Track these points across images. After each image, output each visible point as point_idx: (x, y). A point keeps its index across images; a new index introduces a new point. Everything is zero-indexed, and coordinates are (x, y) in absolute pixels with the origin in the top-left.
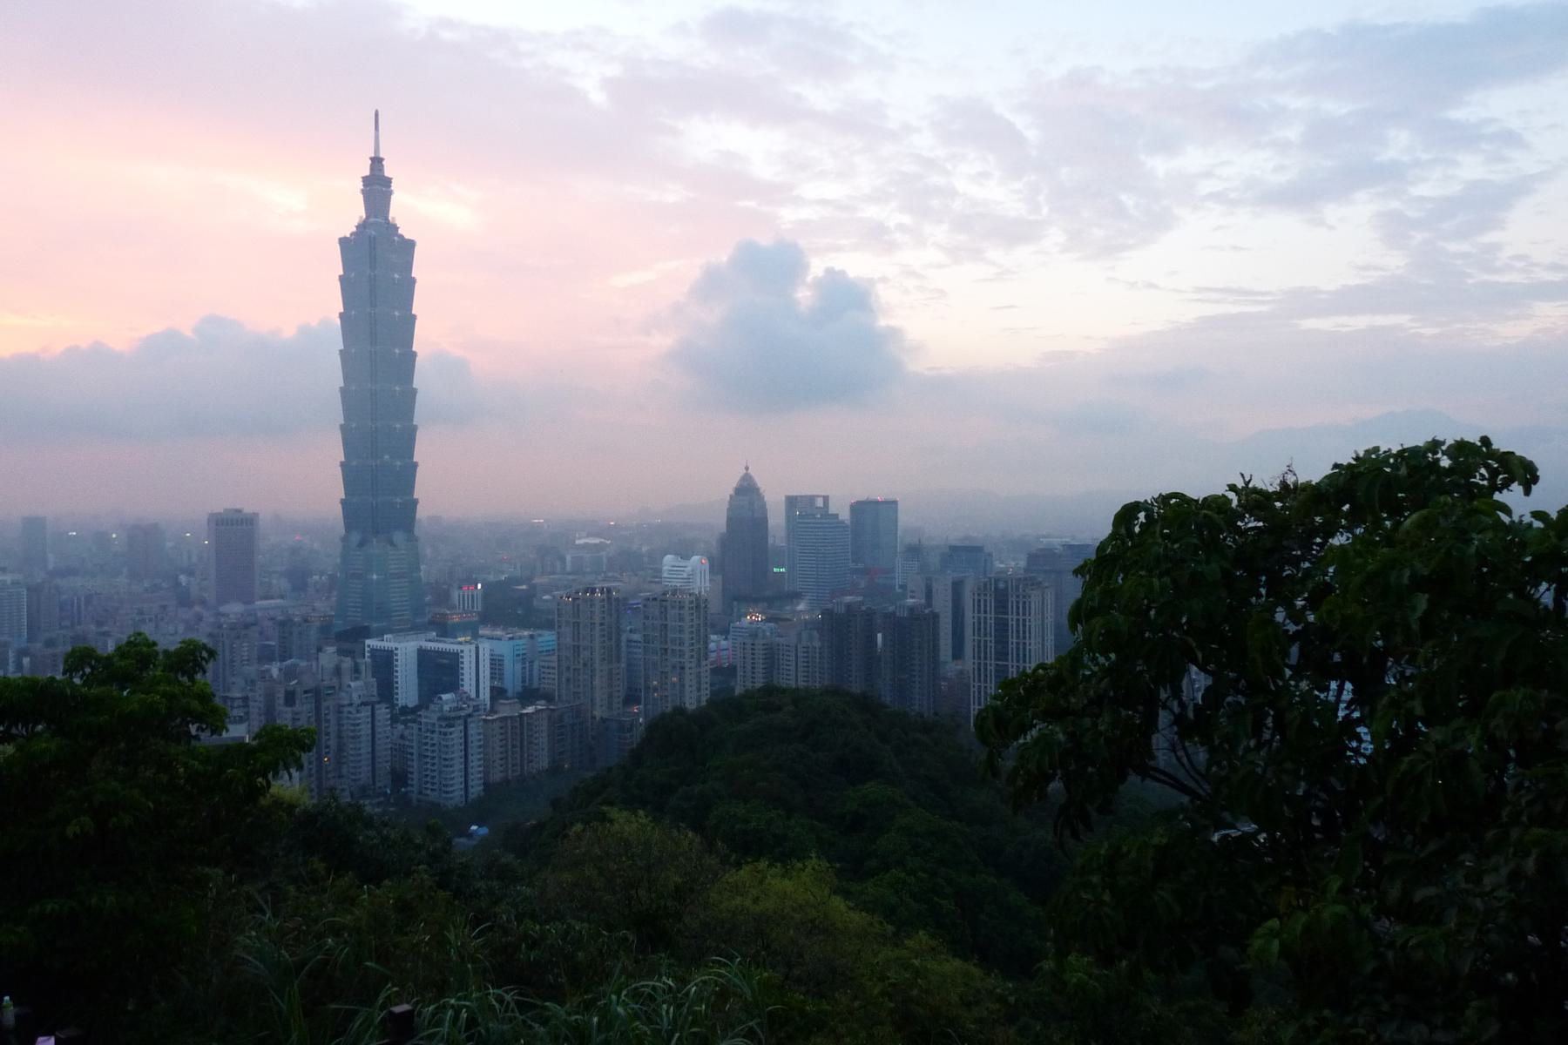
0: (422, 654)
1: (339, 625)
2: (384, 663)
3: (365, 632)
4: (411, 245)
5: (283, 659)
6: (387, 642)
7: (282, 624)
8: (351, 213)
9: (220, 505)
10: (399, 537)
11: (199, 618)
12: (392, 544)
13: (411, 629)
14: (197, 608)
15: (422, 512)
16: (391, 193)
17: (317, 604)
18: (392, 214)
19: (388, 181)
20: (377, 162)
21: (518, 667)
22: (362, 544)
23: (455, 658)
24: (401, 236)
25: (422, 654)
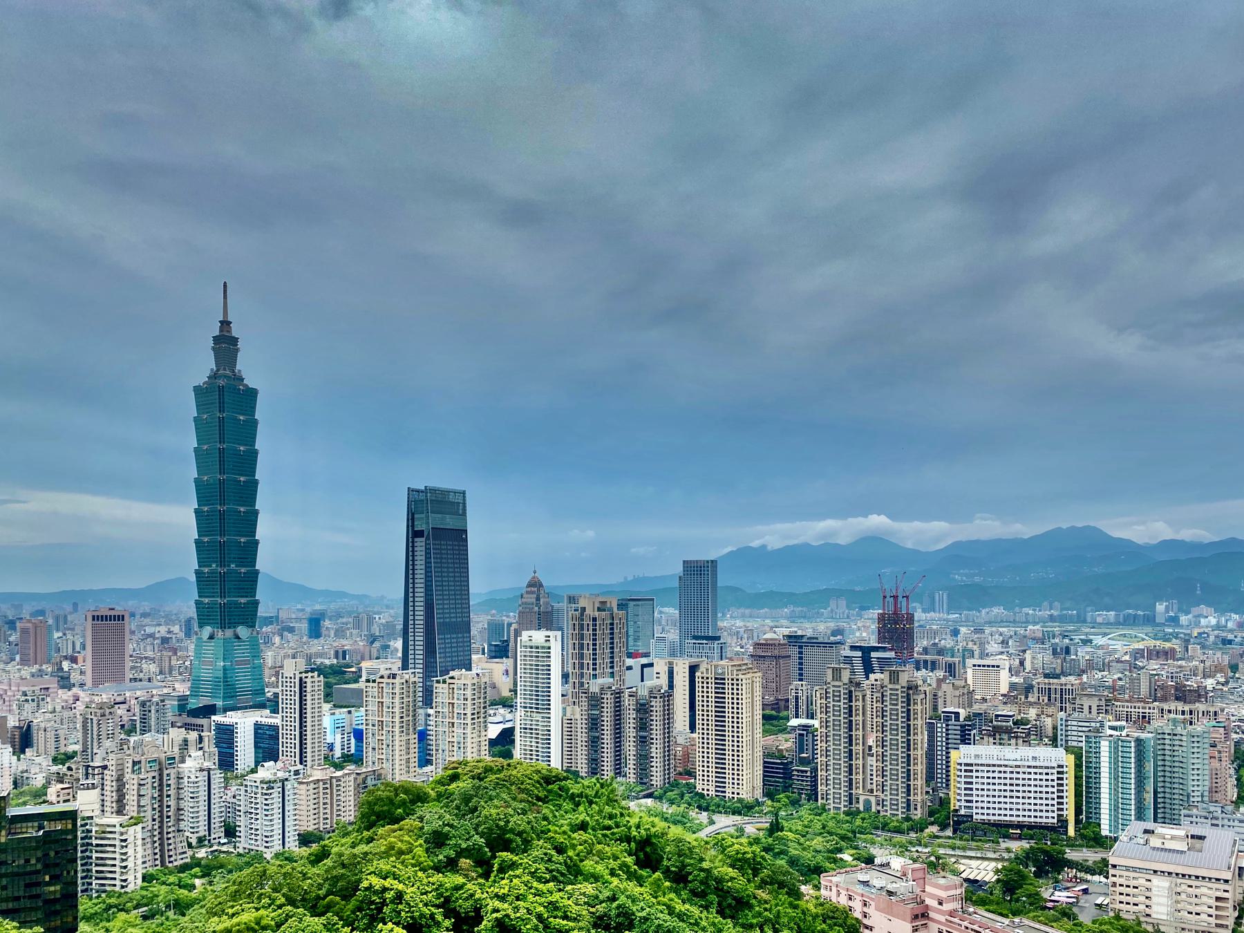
0: (258, 727)
1: (194, 703)
2: (226, 736)
3: (209, 710)
5: (143, 732)
6: (230, 718)
7: (143, 704)
10: (242, 631)
12: (238, 637)
13: (251, 707)
14: (75, 690)
15: (262, 612)
17: (177, 686)
21: (339, 736)
22: (211, 637)
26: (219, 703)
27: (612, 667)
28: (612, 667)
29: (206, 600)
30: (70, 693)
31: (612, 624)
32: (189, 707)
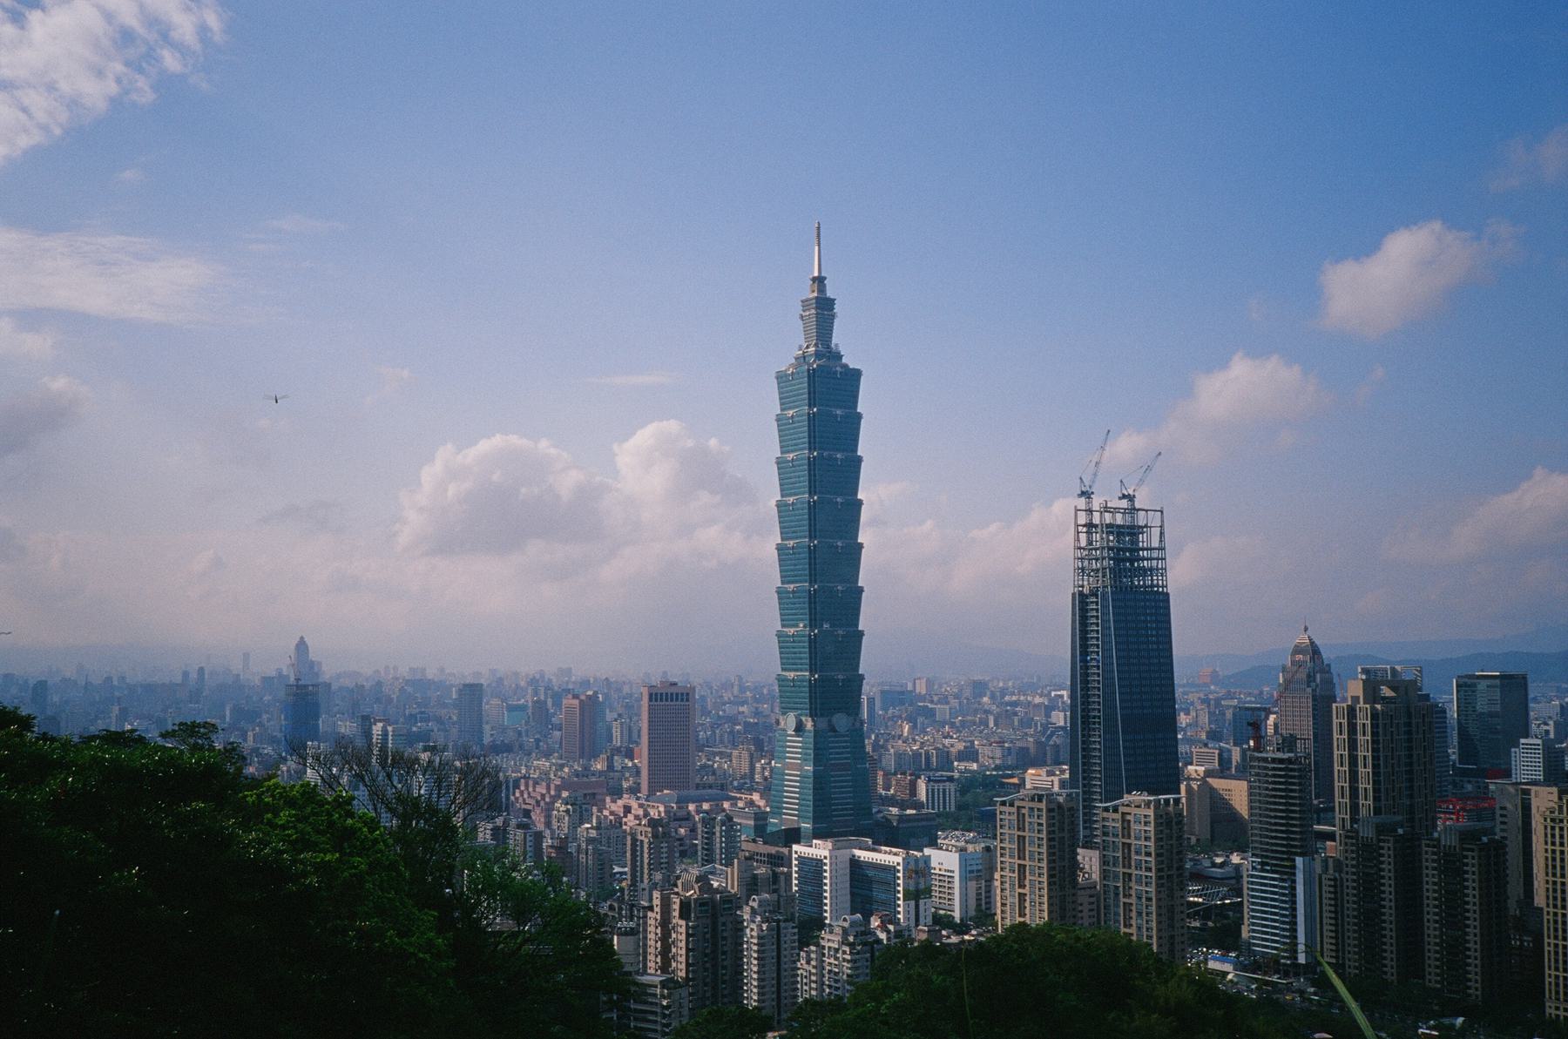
4: (857, 374)
6: (820, 850)
8: (789, 343)
9: (656, 680)
10: (841, 721)
11: (627, 810)
12: (833, 729)
16: (833, 316)
17: (756, 797)
18: (834, 341)
19: (832, 301)
20: (820, 281)
23: (892, 870)
24: (846, 366)
25: (855, 863)
26: (806, 826)
27: (1411, 796)
28: (1411, 796)
29: (791, 675)
30: (620, 802)
31: (1409, 724)
32: (769, 829)
